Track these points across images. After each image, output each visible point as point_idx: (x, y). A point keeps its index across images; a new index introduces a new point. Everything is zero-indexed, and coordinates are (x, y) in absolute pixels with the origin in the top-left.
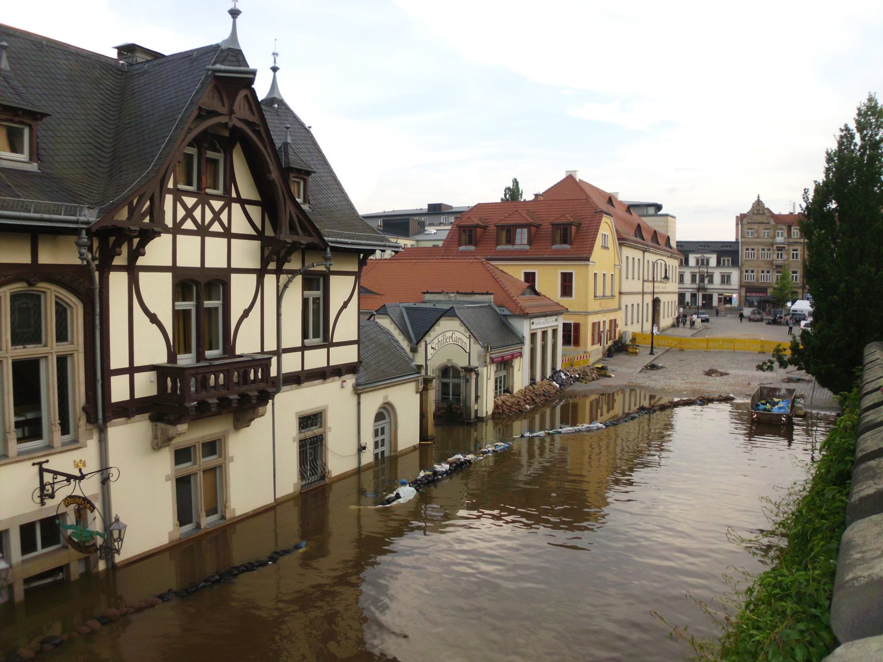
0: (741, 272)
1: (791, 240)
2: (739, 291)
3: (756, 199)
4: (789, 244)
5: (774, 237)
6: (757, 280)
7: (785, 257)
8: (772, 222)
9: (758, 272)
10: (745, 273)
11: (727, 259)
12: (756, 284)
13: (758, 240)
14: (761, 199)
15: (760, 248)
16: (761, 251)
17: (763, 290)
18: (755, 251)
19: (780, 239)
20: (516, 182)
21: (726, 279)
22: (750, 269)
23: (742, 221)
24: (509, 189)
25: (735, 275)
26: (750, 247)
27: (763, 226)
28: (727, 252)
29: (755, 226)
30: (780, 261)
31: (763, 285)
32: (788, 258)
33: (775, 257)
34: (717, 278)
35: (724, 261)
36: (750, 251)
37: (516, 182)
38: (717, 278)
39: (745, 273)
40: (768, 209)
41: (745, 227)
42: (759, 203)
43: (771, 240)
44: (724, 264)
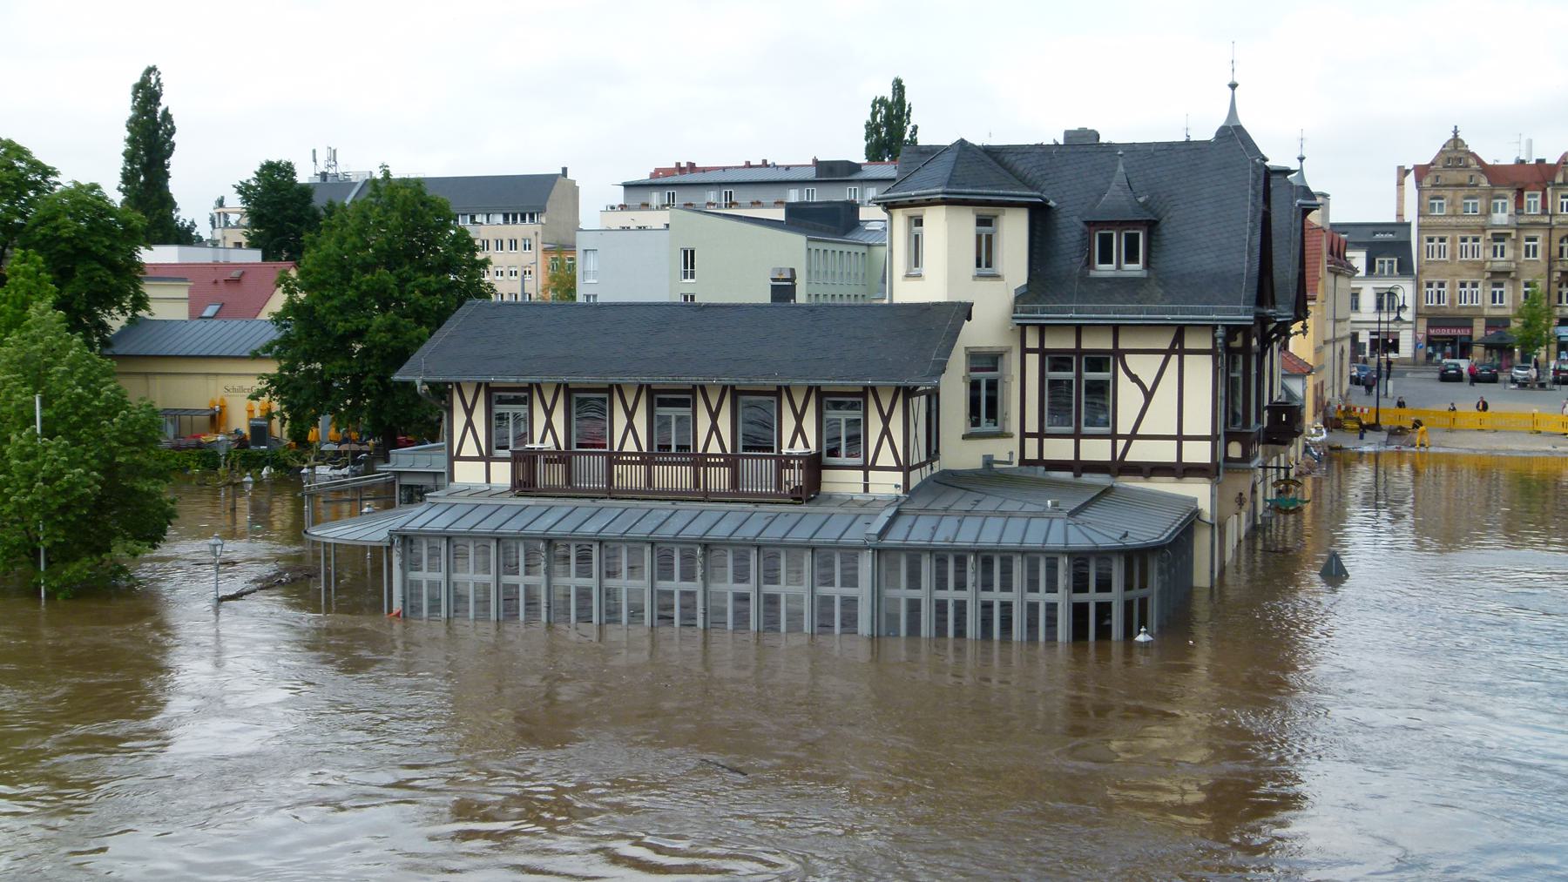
0: (1418, 287)
1: (1523, 220)
2: (1415, 323)
3: (1451, 136)
4: (1520, 228)
5: (1488, 213)
6: (1452, 301)
7: (1509, 253)
8: (1484, 182)
9: (1453, 286)
10: (1425, 289)
11: (1385, 262)
12: (1449, 311)
13: (1453, 221)
14: (1460, 136)
15: (1459, 236)
16: (1459, 244)
17: (1467, 322)
18: (1447, 243)
19: (1501, 218)
20: (899, 87)
21: (1385, 300)
22: (1436, 280)
23: (1419, 181)
24: (882, 101)
25: (1406, 291)
26: (1437, 236)
27: (1466, 191)
28: (1387, 245)
29: (1448, 193)
30: (1500, 264)
31: (1465, 312)
32: (1517, 256)
33: (1489, 253)
34: (1368, 300)
35: (1382, 262)
36: (1436, 243)
37: (899, 87)
38: (1368, 300)
39: (1425, 289)
40: (1474, 155)
41: (1427, 194)
42: (1456, 141)
43: (1481, 220)
44: (1382, 271)
